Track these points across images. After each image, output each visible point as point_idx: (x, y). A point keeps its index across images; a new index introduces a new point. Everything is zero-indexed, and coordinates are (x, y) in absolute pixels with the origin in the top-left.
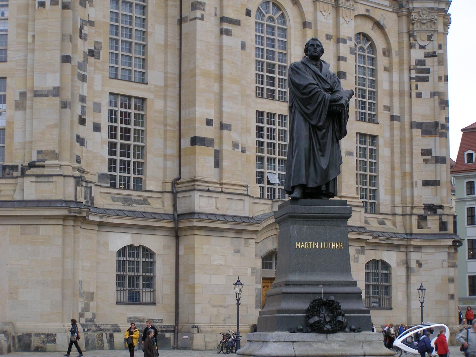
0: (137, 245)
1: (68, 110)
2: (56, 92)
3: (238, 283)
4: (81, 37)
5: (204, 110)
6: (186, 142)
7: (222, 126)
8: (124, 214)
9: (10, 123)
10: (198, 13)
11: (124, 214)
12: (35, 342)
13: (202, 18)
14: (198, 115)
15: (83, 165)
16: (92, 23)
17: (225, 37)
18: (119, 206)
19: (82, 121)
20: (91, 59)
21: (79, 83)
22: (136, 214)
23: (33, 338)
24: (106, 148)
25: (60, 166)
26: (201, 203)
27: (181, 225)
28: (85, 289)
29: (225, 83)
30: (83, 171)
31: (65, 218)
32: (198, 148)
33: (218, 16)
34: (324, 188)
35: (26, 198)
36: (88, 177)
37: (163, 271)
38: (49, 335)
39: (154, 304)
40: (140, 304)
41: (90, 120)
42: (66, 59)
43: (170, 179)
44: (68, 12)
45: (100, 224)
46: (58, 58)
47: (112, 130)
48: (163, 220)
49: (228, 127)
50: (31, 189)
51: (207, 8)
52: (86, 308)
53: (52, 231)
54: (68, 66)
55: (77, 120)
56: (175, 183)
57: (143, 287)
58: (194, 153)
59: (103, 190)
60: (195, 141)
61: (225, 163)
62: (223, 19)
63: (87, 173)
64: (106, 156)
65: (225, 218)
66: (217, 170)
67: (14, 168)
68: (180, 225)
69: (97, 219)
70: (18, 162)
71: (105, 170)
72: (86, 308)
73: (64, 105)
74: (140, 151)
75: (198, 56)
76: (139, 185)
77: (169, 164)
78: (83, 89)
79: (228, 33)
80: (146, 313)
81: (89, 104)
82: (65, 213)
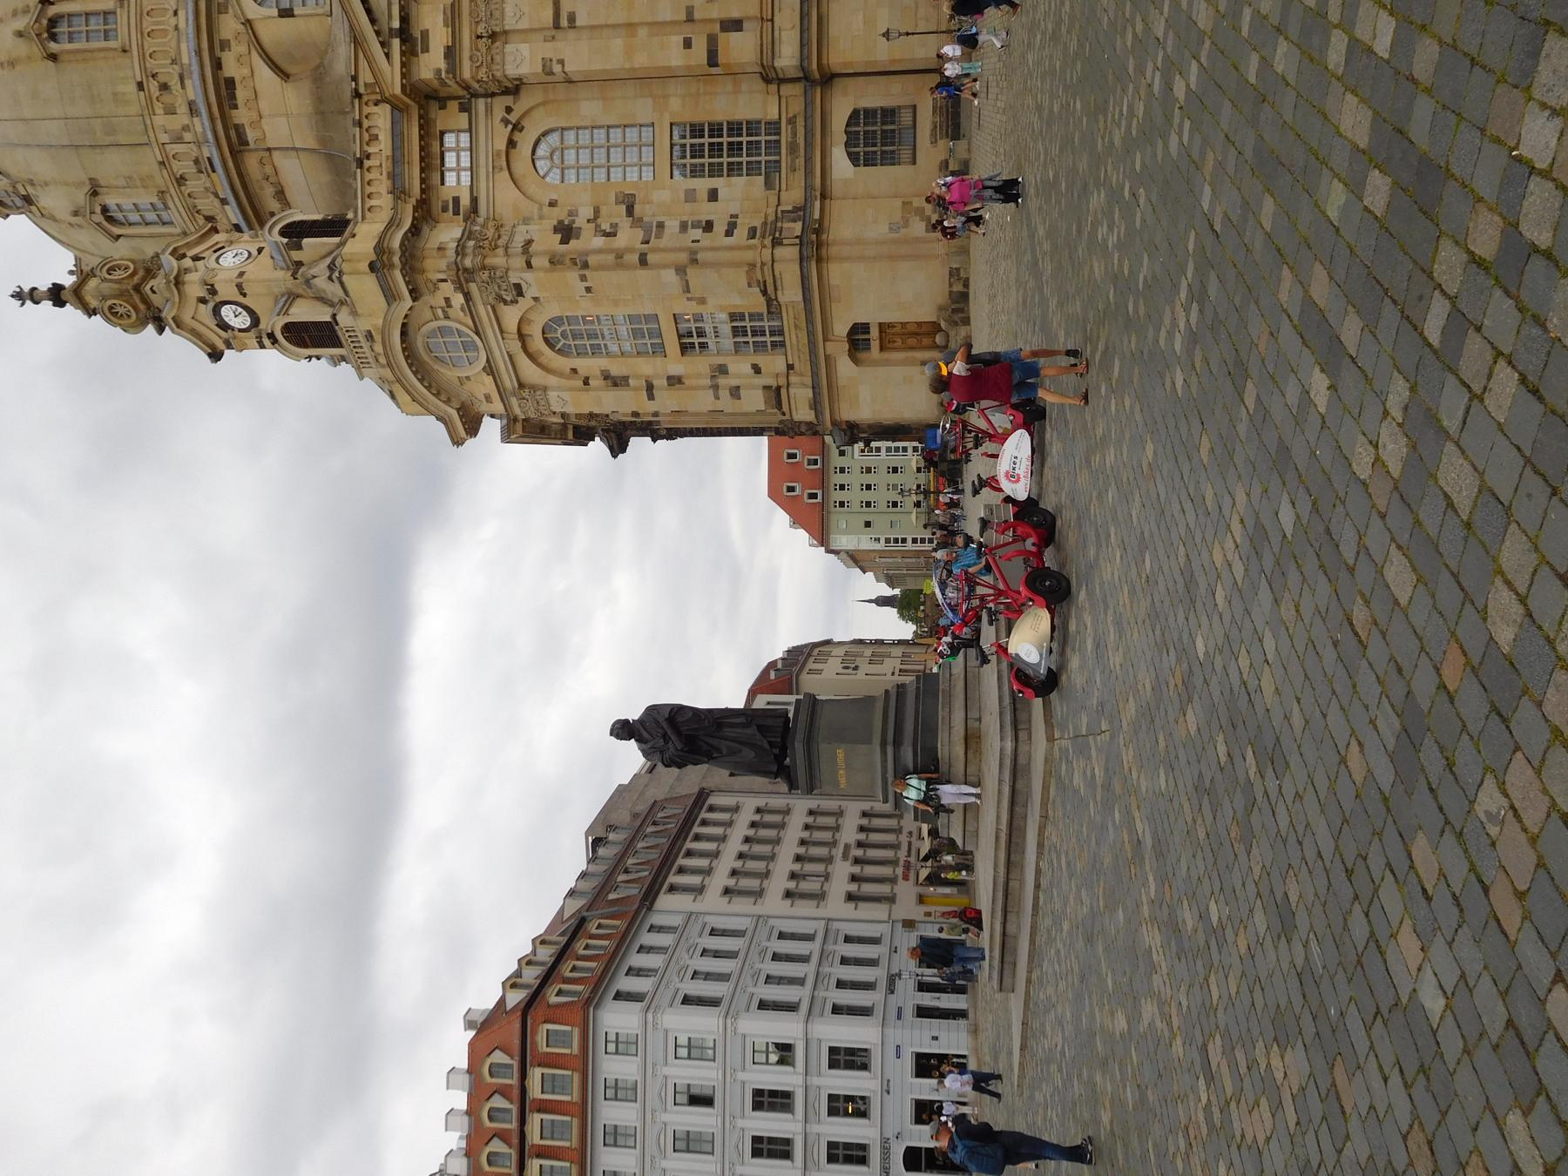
0: (844, 138)
1: (699, 257)
2: (681, 270)
3: (887, 35)
4: (614, 235)
5: (673, 55)
6: (714, 70)
7: (690, 19)
8: (808, 160)
9: (722, 309)
10: (557, 68)
11: (808, 160)
12: (958, 288)
13: (561, 62)
14: (680, 63)
15: (757, 223)
16: (597, 211)
17: (578, 23)
18: (800, 161)
19: (708, 227)
20: (637, 207)
21: (667, 231)
22: (809, 144)
23: (955, 289)
24: (734, 179)
25: (763, 264)
26: (787, 57)
27: (817, 75)
28: (897, 217)
29: (636, 20)
30: (765, 223)
31: (819, 260)
32: (721, 59)
33: (553, 32)
34: (776, 751)
35: (800, 298)
36: (771, 218)
37: (874, 96)
38: (951, 275)
39: (914, 107)
40: (914, 126)
41: (706, 211)
42: (643, 261)
43: (762, 85)
44: (592, 260)
45: (823, 197)
46: (642, 274)
47: (715, 171)
48: (813, 102)
49: (690, 11)
50: (790, 294)
51: (548, 56)
52: (919, 211)
53: (836, 273)
54: (650, 258)
55: (706, 240)
56: (767, 80)
57: (893, 123)
58: (728, 65)
59: (784, 186)
60: (713, 60)
61: (735, 14)
62: (557, 26)
63: (766, 217)
64: (744, 178)
65: (804, 16)
66: (745, 25)
67: (769, 306)
68: (819, 79)
69: (817, 204)
70: (762, 300)
71: (762, 178)
72: (919, 211)
73: (694, 261)
74: (735, 128)
75: (608, 67)
76: (774, 128)
77: (744, 87)
78: (672, 225)
79: (572, 18)
80: (926, 119)
81: (689, 212)
82: (814, 264)
